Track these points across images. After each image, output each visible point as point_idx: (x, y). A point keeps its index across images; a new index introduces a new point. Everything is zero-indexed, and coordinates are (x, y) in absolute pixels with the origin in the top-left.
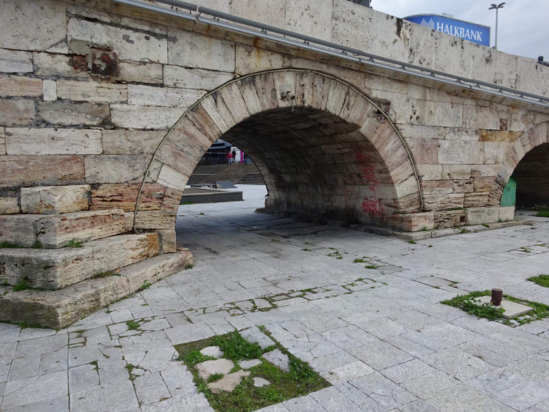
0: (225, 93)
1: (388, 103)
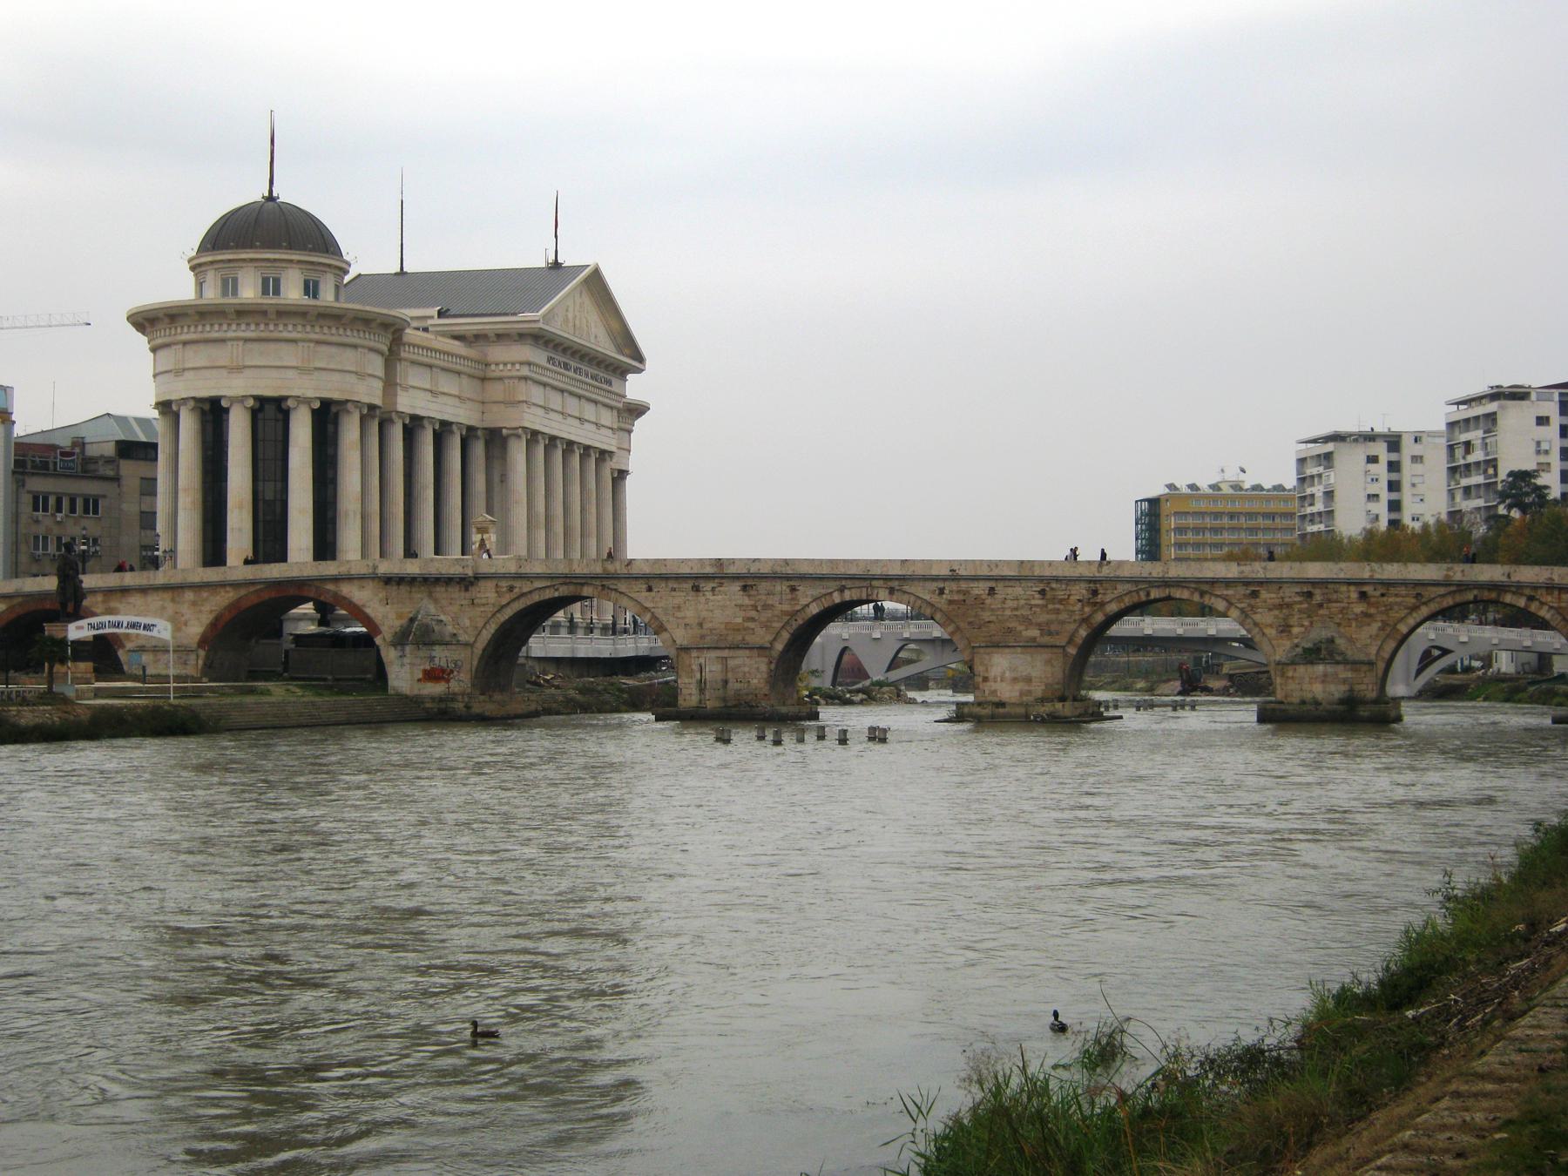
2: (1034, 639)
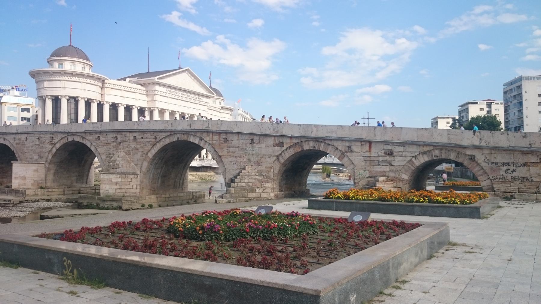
0: (418, 157)
1: (474, 156)
2: (37, 160)
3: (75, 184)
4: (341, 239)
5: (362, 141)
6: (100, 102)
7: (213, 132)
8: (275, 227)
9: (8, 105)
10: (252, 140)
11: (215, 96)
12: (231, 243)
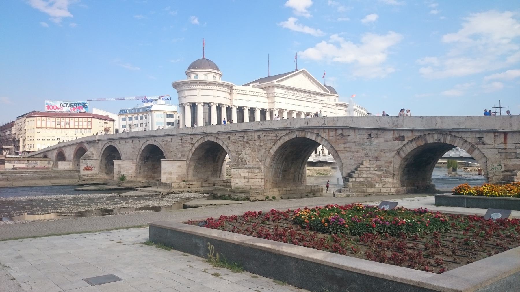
2: (180, 158)
3: (210, 178)
4: (479, 238)
5: (495, 133)
6: (229, 106)
7: (329, 129)
8: (403, 224)
9: (156, 113)
10: (370, 135)
11: (329, 93)
12: (357, 237)
